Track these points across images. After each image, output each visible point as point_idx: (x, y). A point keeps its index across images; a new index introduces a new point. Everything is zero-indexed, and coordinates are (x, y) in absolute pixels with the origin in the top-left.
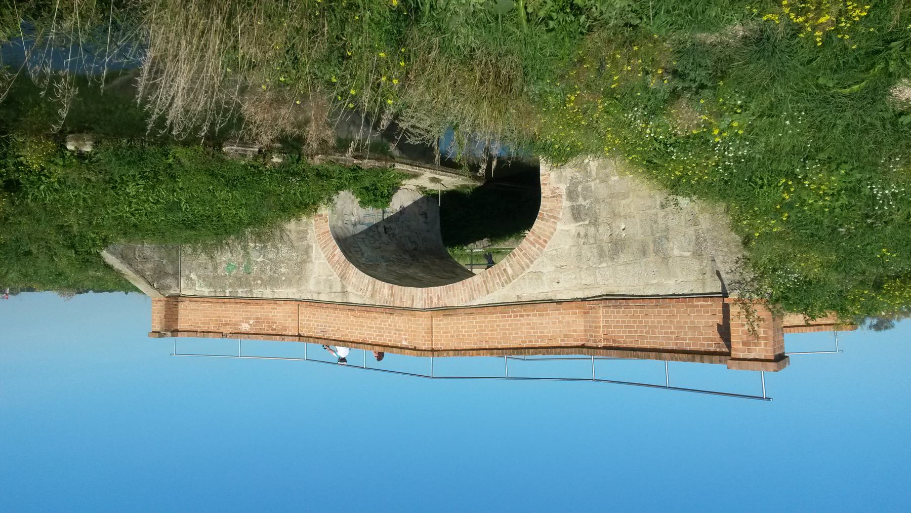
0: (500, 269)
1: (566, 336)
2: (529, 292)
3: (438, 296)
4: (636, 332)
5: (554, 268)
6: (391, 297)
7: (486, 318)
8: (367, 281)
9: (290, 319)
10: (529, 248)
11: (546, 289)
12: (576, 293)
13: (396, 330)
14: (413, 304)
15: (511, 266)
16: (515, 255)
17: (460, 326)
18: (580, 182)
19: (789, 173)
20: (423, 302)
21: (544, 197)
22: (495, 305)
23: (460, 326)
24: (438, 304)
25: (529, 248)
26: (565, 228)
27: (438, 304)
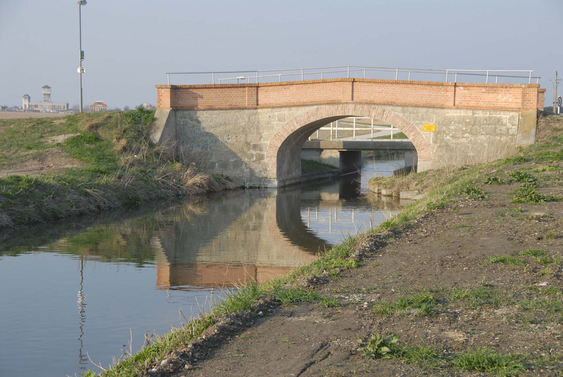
0: (300, 124)
1: (267, 91)
2: (285, 112)
3: (338, 111)
4: (226, 95)
5: (272, 123)
6: (370, 111)
7: (309, 99)
8: (387, 120)
9: (449, 96)
10: (284, 133)
11: (276, 113)
12: (261, 111)
13: (368, 92)
14: (355, 107)
15: (294, 126)
16: (292, 130)
17: (304, 96)
18: (254, 162)
19: (166, 155)
20: (348, 107)
21: (275, 157)
22: (303, 106)
23: (304, 96)
24: (338, 106)
25: (284, 133)
26: (266, 142)
27: (338, 106)
